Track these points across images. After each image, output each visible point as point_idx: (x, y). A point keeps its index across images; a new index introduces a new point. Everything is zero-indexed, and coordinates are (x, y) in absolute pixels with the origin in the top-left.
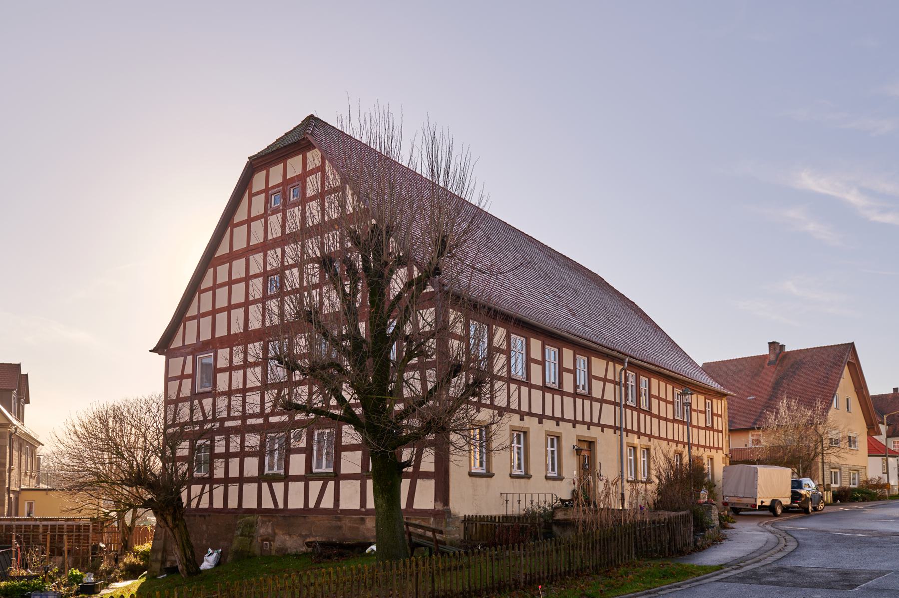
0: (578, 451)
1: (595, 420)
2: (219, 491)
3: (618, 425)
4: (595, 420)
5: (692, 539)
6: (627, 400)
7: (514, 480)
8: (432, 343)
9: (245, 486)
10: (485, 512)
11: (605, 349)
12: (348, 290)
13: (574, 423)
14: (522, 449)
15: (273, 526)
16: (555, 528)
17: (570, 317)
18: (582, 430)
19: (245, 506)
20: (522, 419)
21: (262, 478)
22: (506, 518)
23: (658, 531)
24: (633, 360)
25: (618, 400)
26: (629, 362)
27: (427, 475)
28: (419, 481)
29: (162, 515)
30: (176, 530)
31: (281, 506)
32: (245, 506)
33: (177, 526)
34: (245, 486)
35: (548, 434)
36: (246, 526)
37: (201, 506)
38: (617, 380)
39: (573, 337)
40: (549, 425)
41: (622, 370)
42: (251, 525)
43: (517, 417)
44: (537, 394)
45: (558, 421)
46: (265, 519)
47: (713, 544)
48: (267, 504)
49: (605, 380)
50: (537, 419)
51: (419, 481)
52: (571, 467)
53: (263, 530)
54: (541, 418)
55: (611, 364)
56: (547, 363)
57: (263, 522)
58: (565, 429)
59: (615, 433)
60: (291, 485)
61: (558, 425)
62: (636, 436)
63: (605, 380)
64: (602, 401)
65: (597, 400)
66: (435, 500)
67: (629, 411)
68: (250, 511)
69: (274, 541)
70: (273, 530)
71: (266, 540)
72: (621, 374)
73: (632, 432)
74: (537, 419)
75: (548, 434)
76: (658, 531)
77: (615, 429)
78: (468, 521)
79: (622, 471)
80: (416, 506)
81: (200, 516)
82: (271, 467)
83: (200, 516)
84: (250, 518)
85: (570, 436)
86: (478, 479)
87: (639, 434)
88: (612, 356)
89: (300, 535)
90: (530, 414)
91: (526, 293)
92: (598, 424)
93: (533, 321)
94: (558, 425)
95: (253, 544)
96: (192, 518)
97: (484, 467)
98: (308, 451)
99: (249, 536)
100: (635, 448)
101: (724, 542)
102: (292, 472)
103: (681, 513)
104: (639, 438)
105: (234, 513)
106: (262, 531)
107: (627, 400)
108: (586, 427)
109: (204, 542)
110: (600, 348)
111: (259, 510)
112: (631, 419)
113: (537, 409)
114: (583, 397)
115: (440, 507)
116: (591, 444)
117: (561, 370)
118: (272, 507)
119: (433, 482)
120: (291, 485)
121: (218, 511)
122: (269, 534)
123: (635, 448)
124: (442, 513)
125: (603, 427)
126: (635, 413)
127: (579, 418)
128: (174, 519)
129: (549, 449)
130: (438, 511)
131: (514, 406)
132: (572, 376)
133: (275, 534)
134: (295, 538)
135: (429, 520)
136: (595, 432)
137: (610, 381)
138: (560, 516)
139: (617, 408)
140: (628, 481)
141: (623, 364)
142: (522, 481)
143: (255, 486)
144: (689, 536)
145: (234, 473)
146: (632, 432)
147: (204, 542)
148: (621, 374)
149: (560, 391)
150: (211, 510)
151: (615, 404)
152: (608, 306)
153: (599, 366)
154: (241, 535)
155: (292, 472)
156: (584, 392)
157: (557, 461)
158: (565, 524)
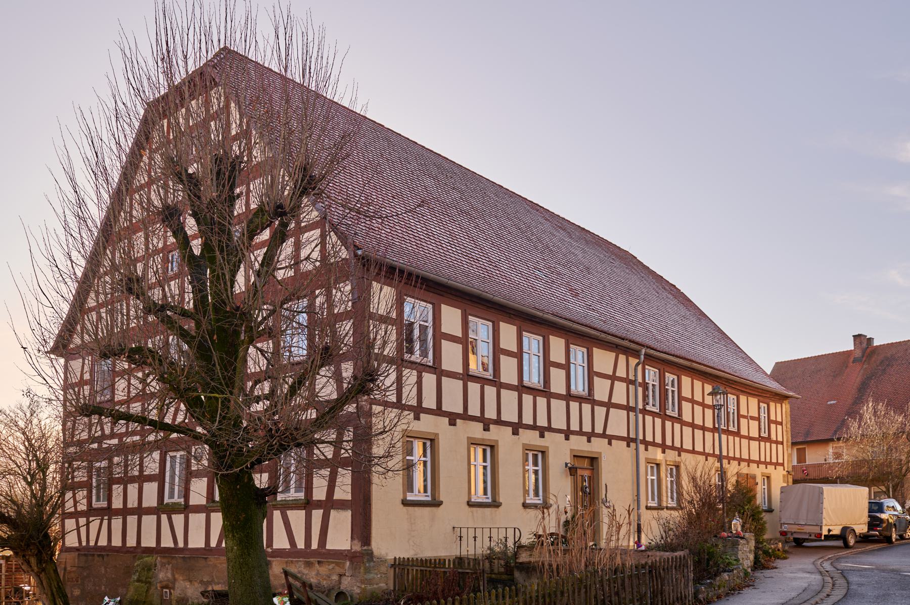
0: (572, 471)
1: (599, 429)
2: (117, 523)
3: (632, 435)
4: (599, 429)
5: (691, 590)
6: (646, 403)
7: (474, 509)
8: (346, 327)
9: (144, 518)
10: (428, 553)
11: (609, 337)
12: (197, 251)
13: (568, 434)
14: (489, 469)
15: (173, 571)
16: (517, 574)
17: (569, 297)
18: (579, 444)
19: (143, 545)
20: (486, 429)
21: (163, 509)
22: (460, 560)
23: (635, 581)
24: (652, 352)
25: (632, 404)
26: (645, 354)
27: (342, 505)
28: (333, 513)
29: (24, 556)
30: (43, 575)
31: (181, 544)
32: (143, 545)
33: (44, 570)
34: (144, 518)
35: (527, 448)
36: (143, 569)
37: (99, 544)
38: (631, 377)
39: (561, 321)
40: (529, 437)
41: (638, 364)
42: (149, 568)
43: (480, 426)
44: (558, 406)
45: (542, 431)
46: (164, 561)
47: (727, 595)
48: (167, 542)
49: (613, 378)
50: (510, 429)
51: (333, 513)
52: (562, 491)
53: (163, 575)
54: (516, 427)
55: (622, 358)
56: (525, 356)
57: (163, 565)
58: (552, 441)
59: (628, 446)
60: (192, 516)
61: (542, 436)
62: (659, 450)
63: (613, 378)
64: (609, 405)
65: (601, 404)
66: (352, 538)
67: (649, 419)
68: (149, 551)
69: (174, 589)
70: (173, 575)
71: (167, 587)
72: (636, 370)
73: (654, 444)
74: (510, 429)
75: (527, 448)
76: (635, 581)
77: (629, 441)
78: (400, 566)
79: (638, 495)
80: (329, 546)
81: (99, 555)
82: (171, 495)
83: (99, 555)
84: (148, 559)
85: (561, 452)
86: (416, 509)
87: (664, 447)
88: (623, 346)
89: (202, 582)
90: (499, 422)
91: (504, 266)
92: (603, 435)
93: (498, 299)
94: (542, 436)
95: (151, 591)
96: (90, 558)
97: (429, 493)
98: (160, 478)
99: (146, 583)
100: (658, 465)
101: (746, 590)
102: (192, 502)
103: (678, 554)
104: (664, 452)
105: (131, 552)
106: (161, 576)
107: (646, 403)
108: (585, 438)
109: (103, 588)
110: (603, 335)
111: (158, 550)
112: (652, 428)
113: (510, 415)
114: (580, 399)
115: (357, 547)
116: (594, 461)
117: (548, 364)
118: (172, 545)
119: (349, 513)
120: (192, 516)
121: (117, 550)
122: (168, 580)
123: (658, 465)
124: (361, 557)
125: (611, 439)
126: (658, 421)
127: (575, 426)
128: (40, 562)
129: (531, 467)
130: (355, 552)
131: (474, 410)
132: (515, 361)
133: (175, 579)
134: (196, 585)
135: (344, 563)
136: (598, 446)
137: (621, 379)
138: (524, 557)
139: (632, 414)
140: (648, 508)
141: (638, 357)
142: (487, 511)
143: (202, 516)
144: (686, 586)
145: (132, 503)
146: (654, 444)
147: (103, 588)
148: (636, 370)
149: (545, 392)
150: (109, 549)
151: (628, 408)
152: (634, 288)
153: (604, 360)
154: (138, 581)
155: (192, 502)
156: (583, 393)
157: (543, 485)
158: (528, 569)
